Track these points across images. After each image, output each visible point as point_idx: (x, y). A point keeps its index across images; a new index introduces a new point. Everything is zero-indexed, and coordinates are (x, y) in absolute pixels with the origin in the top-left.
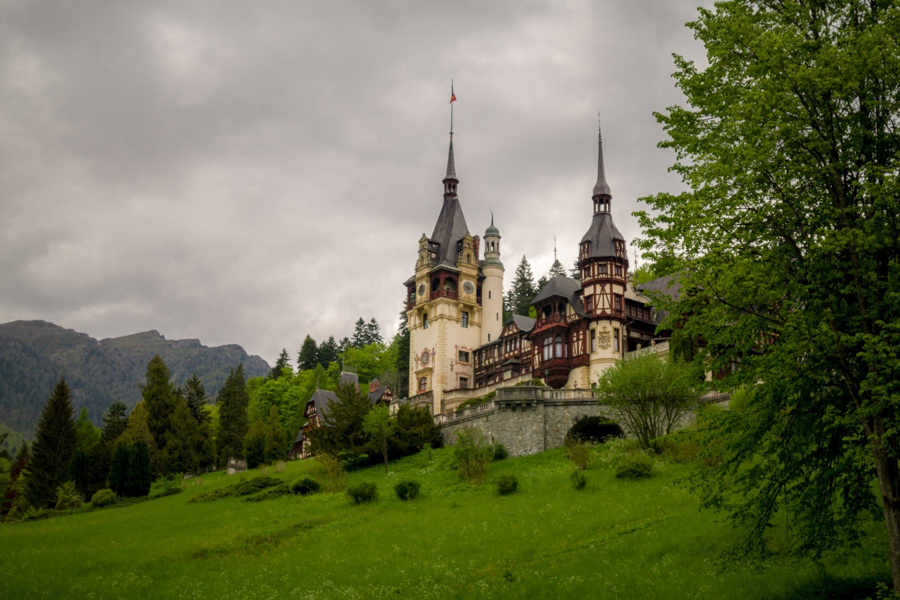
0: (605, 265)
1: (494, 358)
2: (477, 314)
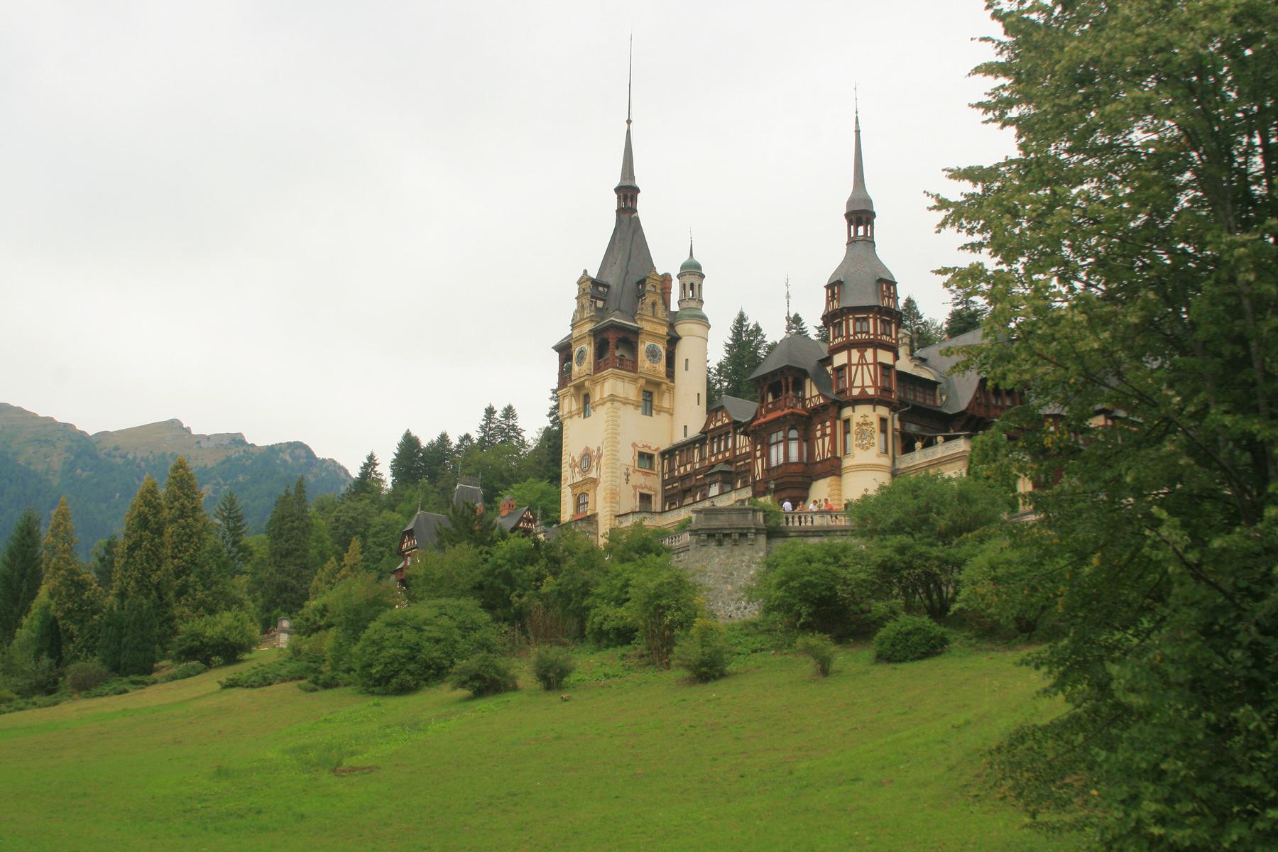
0: (866, 319)
1: (692, 462)
2: (667, 395)
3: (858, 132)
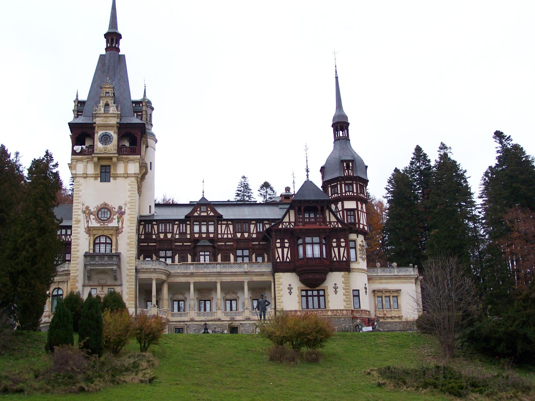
0: (363, 186)
1: (172, 233)
3: (337, 78)
